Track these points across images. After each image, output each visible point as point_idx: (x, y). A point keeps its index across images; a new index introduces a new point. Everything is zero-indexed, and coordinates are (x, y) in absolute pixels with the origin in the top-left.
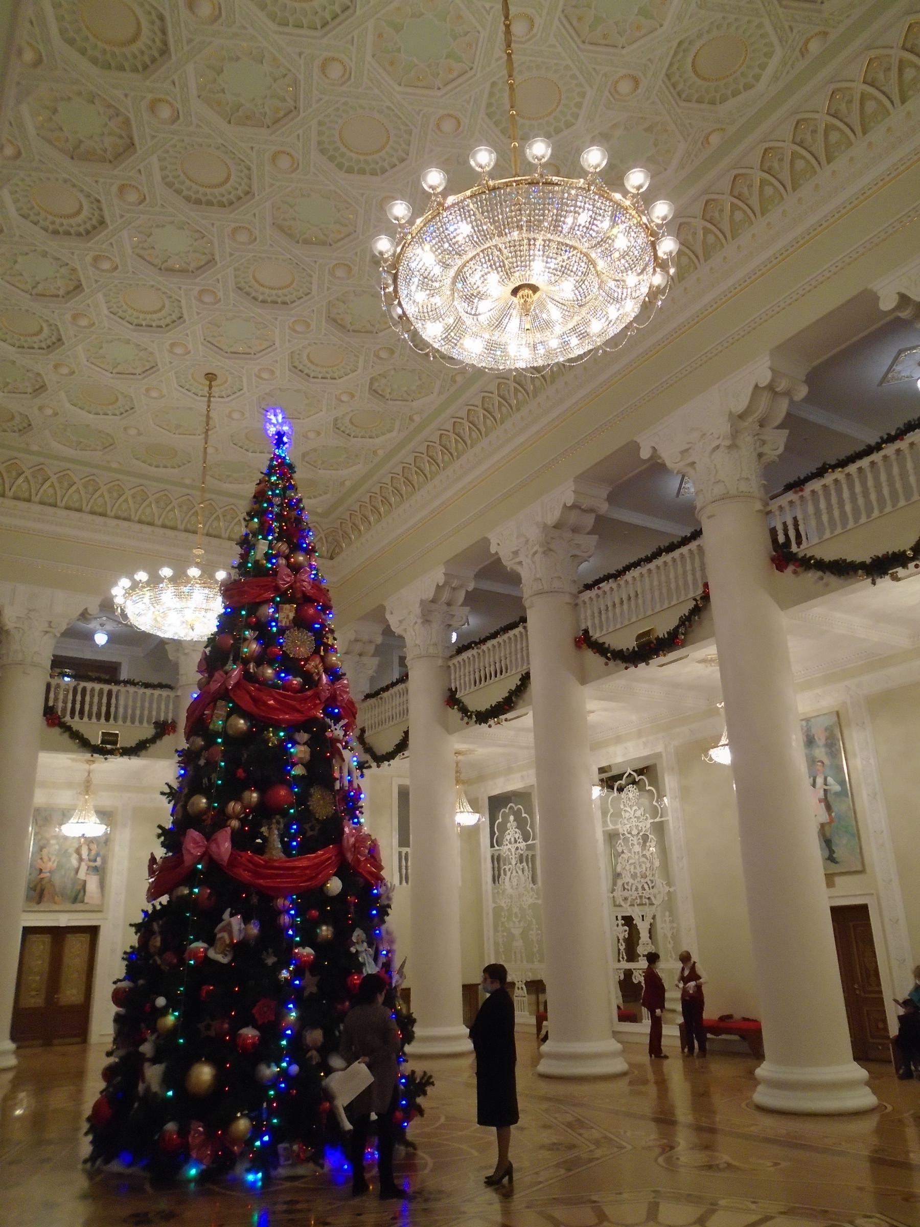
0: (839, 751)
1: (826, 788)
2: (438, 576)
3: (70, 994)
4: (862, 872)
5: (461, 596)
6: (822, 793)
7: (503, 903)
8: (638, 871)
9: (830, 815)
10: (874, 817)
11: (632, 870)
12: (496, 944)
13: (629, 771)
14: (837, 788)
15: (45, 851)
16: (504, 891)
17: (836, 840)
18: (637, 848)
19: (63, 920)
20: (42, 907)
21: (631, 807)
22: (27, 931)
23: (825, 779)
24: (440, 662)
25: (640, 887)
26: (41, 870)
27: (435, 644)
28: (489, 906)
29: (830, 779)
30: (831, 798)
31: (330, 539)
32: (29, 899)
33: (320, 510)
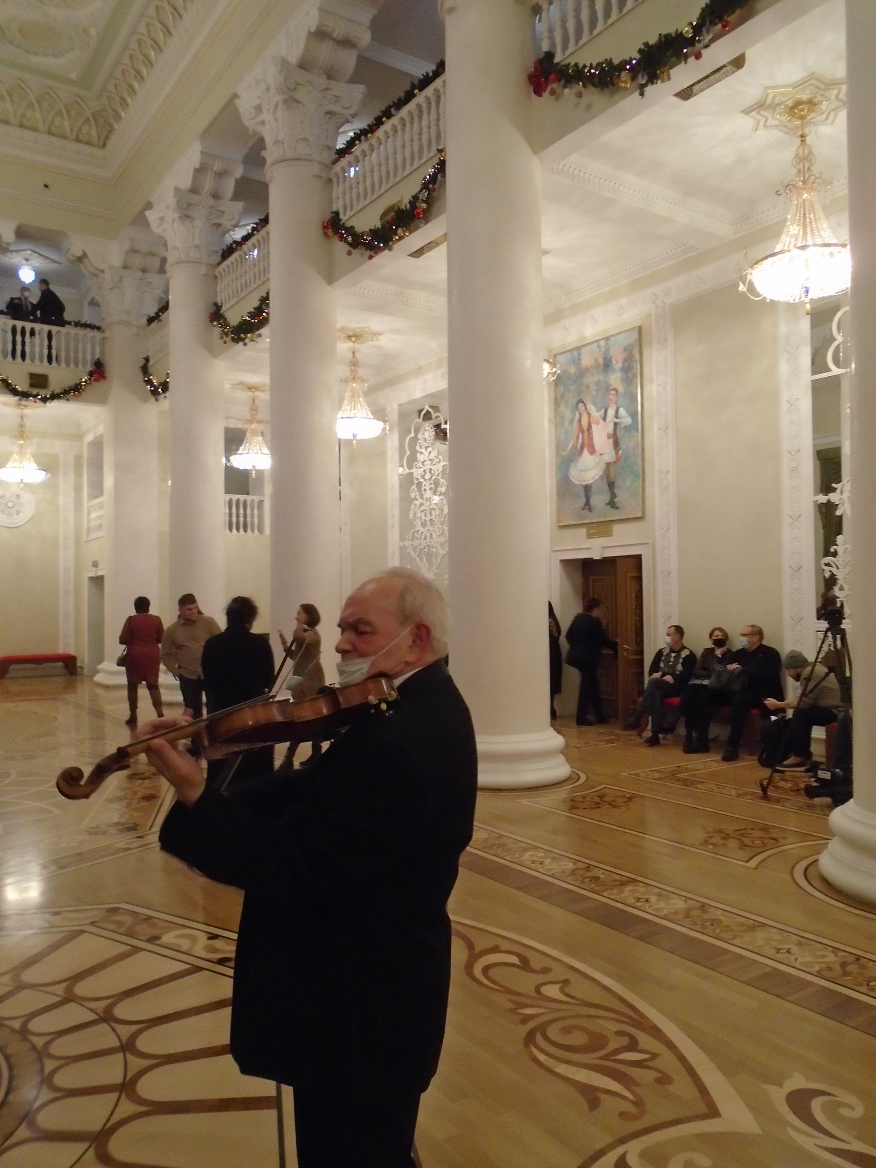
0: (634, 375)
1: (617, 420)
2: (192, 157)
4: (641, 518)
5: (229, 187)
6: (611, 426)
9: (617, 453)
10: (661, 454)
11: (423, 518)
13: (427, 408)
14: (628, 421)
17: (619, 483)
21: (427, 448)
23: (617, 411)
24: (203, 270)
25: (428, 535)
27: (196, 247)
30: (619, 434)
33: (73, 76)
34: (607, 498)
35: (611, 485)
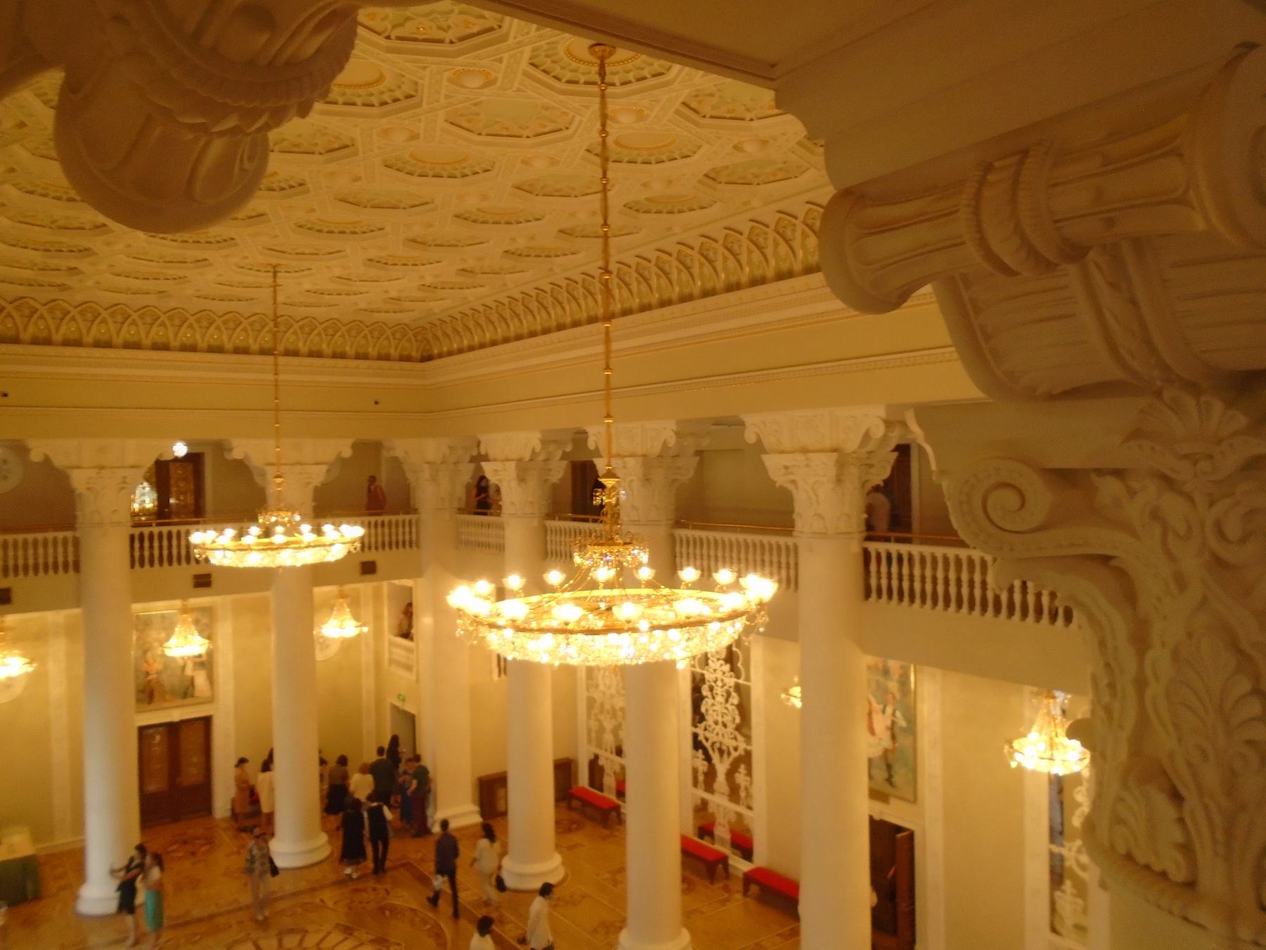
3: (191, 774)
7: (597, 695)
8: (720, 719)
12: (589, 731)
14: (902, 723)
15: (149, 655)
16: (597, 686)
18: (720, 699)
19: (176, 715)
20: (152, 706)
22: (142, 730)
26: (148, 674)
28: (582, 694)
29: (898, 714)
30: (897, 731)
31: (419, 338)
32: (139, 701)
34: (886, 775)
35: (889, 767)
